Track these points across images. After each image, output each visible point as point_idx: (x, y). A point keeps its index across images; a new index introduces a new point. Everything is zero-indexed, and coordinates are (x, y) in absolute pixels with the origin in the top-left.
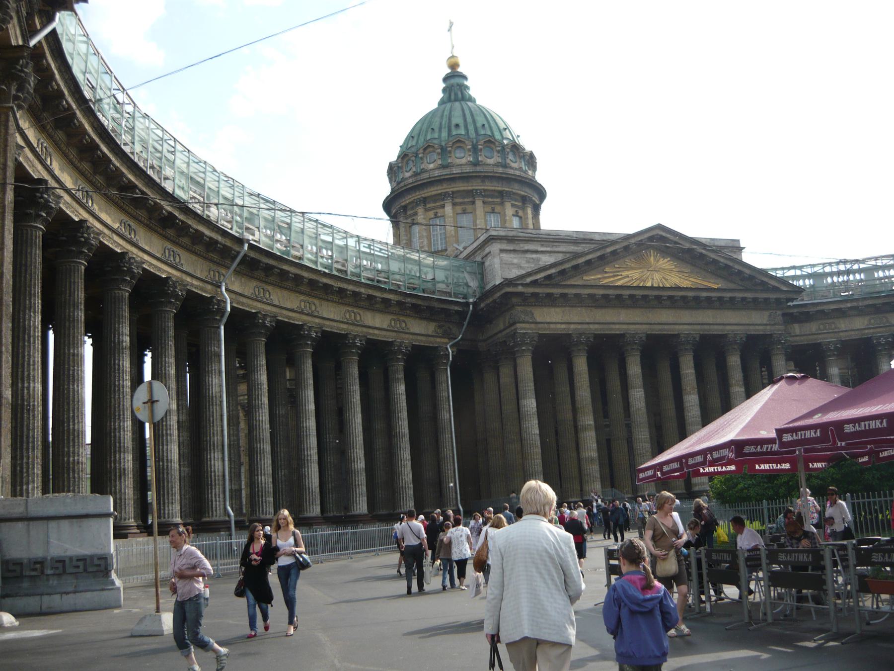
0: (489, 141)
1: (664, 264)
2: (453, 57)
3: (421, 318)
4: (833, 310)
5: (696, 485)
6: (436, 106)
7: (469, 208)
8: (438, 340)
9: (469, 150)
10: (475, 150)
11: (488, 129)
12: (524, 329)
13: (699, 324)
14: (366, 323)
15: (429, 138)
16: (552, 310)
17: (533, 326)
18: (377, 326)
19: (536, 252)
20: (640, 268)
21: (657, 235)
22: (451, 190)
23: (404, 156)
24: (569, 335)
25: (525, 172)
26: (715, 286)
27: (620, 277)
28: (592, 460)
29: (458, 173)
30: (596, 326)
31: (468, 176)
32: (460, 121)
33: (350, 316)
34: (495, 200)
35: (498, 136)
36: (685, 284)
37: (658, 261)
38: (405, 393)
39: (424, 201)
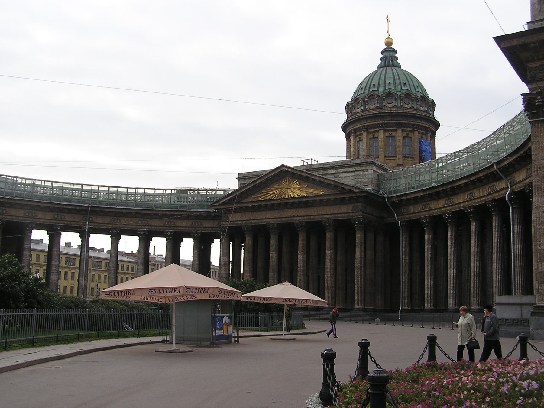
1: (293, 184)
2: (389, 38)
11: (377, 86)
13: (307, 216)
14: (177, 225)
16: (237, 214)
20: (280, 188)
21: (283, 170)
22: (353, 128)
25: (401, 107)
27: (269, 194)
30: (255, 221)
31: (384, 115)
33: (168, 223)
34: (375, 130)
36: (304, 194)
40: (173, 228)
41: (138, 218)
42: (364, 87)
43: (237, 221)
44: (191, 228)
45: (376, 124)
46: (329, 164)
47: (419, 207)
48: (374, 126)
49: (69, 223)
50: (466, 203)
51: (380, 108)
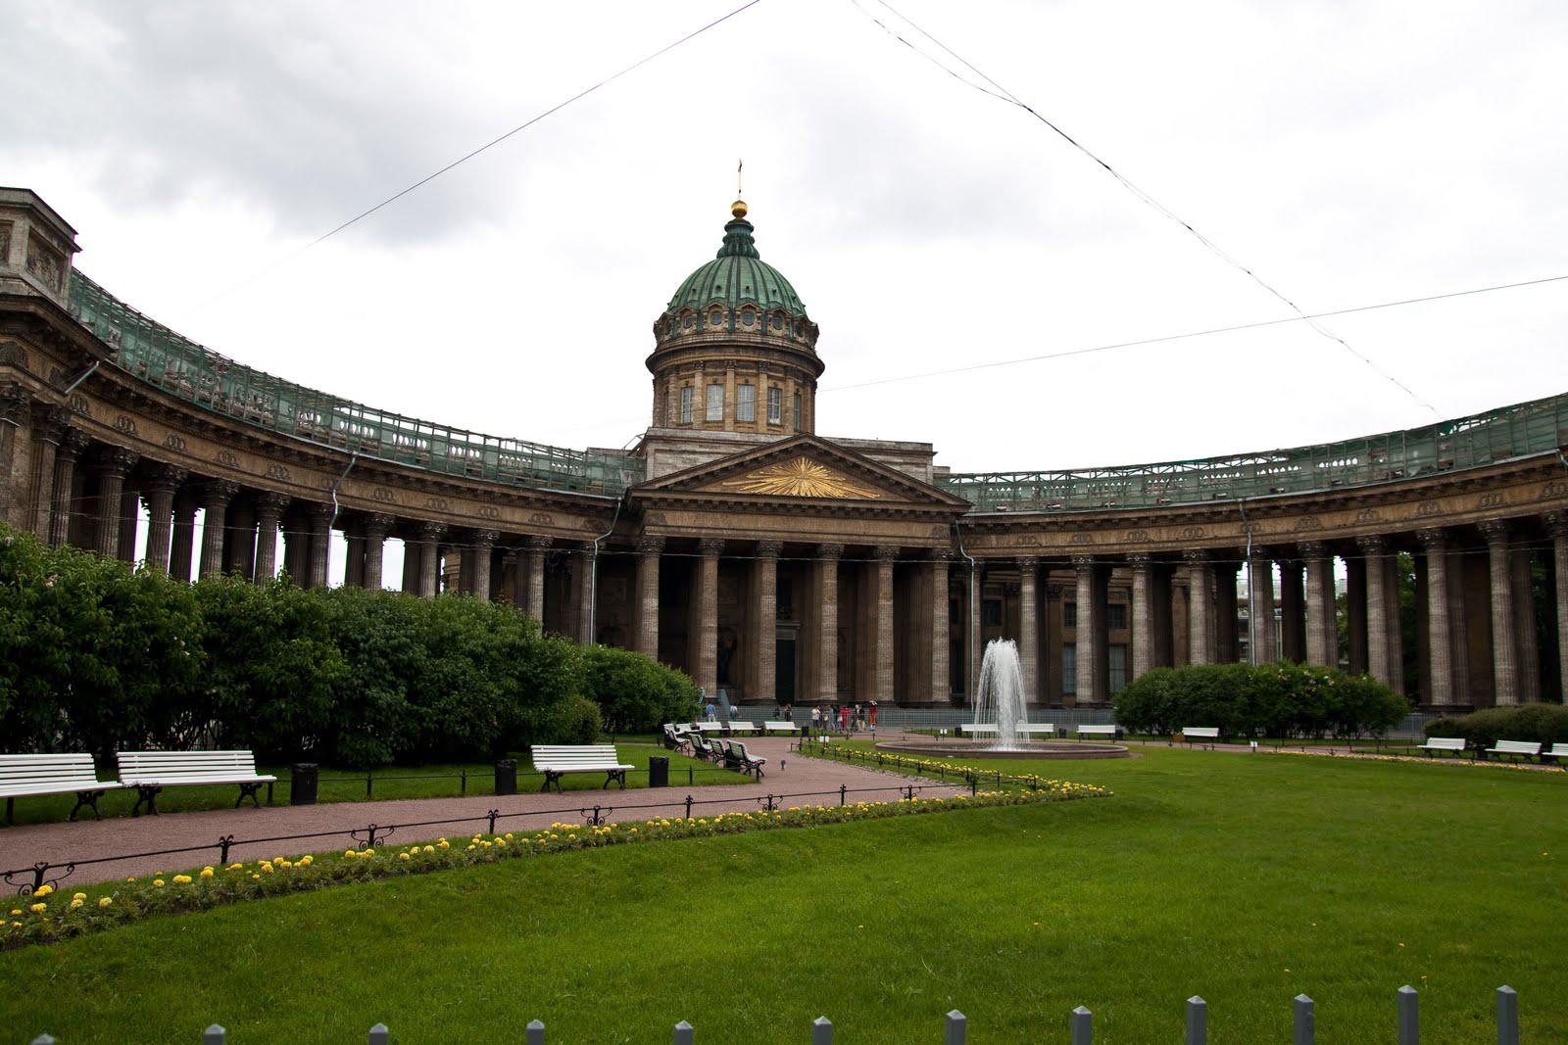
0: (750, 306)
2: (740, 202)
3: (568, 514)
4: (1030, 524)
5: (821, 694)
6: (714, 257)
7: (720, 379)
8: (586, 534)
9: (726, 316)
10: (733, 316)
11: (753, 292)
12: (654, 531)
14: (504, 518)
15: (689, 299)
16: (686, 514)
17: (662, 529)
18: (517, 520)
19: (694, 453)
23: (664, 317)
24: (697, 540)
25: (793, 341)
26: (873, 497)
28: (708, 661)
29: (711, 342)
30: (730, 532)
32: (723, 283)
33: (486, 510)
35: (762, 300)
36: (838, 493)
37: (810, 469)
38: (542, 583)
39: (678, 368)
40: (496, 524)
41: (430, 493)
42: (724, 287)
43: (687, 527)
44: (531, 528)
45: (753, 362)
46: (853, 443)
47: (1011, 539)
48: (746, 364)
49: (296, 489)
50: (1127, 546)
51: (764, 334)
